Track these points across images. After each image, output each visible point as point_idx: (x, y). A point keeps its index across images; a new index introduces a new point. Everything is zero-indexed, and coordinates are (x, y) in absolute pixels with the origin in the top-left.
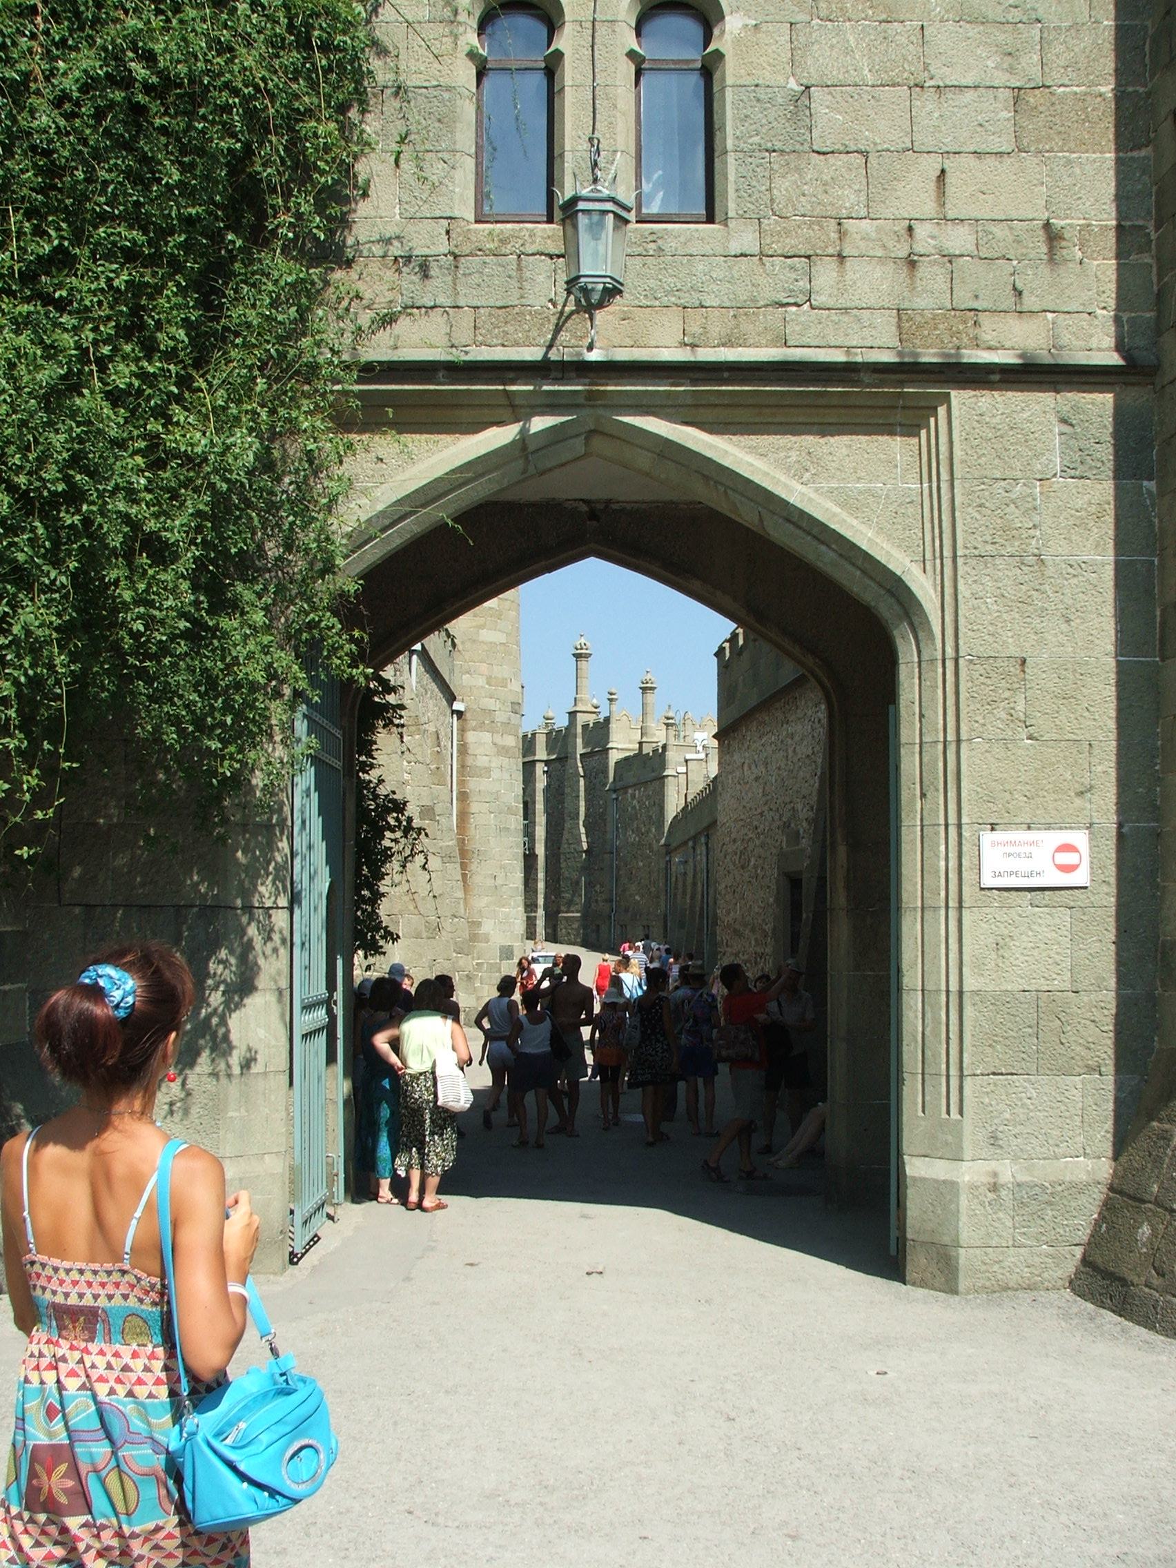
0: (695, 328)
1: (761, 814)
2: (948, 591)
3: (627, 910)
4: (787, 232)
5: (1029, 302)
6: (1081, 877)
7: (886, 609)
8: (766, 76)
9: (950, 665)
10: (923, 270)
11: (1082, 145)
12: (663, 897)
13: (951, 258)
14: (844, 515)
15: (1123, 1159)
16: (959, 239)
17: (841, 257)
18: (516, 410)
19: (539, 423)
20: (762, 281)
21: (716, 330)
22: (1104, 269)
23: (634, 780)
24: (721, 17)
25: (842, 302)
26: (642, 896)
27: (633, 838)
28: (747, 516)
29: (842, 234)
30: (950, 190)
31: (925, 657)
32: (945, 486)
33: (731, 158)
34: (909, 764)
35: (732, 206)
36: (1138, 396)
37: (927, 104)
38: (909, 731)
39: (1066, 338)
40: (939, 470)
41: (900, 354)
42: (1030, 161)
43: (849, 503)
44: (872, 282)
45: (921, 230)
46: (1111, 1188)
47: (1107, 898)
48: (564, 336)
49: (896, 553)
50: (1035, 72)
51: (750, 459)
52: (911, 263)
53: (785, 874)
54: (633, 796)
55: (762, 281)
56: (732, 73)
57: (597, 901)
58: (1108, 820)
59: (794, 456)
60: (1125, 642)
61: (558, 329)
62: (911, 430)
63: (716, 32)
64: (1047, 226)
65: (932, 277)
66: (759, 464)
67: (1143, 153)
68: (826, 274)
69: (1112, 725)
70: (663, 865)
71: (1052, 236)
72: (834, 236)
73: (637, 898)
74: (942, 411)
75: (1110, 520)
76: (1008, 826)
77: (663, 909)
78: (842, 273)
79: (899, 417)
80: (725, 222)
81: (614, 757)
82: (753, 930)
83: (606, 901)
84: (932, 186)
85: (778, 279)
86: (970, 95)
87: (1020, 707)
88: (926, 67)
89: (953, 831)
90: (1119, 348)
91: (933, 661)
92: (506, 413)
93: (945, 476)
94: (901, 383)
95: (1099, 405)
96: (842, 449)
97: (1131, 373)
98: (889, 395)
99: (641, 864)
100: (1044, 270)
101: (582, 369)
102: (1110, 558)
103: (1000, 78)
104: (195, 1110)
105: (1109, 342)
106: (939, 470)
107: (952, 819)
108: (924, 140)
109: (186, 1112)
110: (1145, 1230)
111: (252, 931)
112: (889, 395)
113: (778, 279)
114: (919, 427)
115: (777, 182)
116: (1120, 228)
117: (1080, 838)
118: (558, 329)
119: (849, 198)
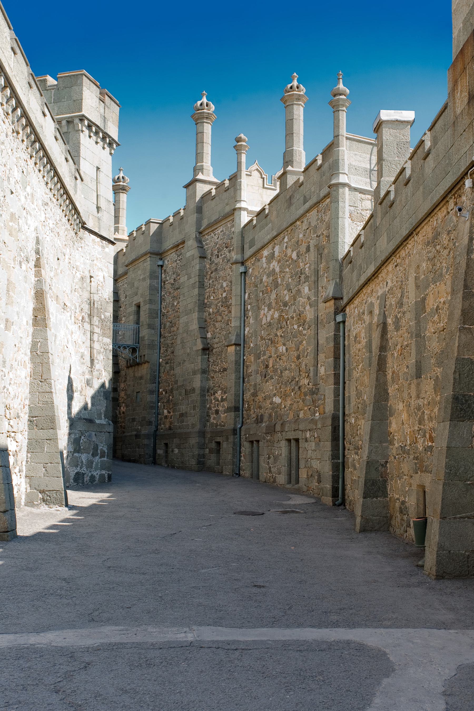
3: (259, 420)
12: (328, 390)
23: (269, 237)
26: (284, 396)
27: (268, 315)
54: (272, 257)
57: (217, 412)
70: (326, 333)
73: (277, 400)
77: (329, 408)
81: (245, 218)
83: (228, 410)
99: (282, 349)
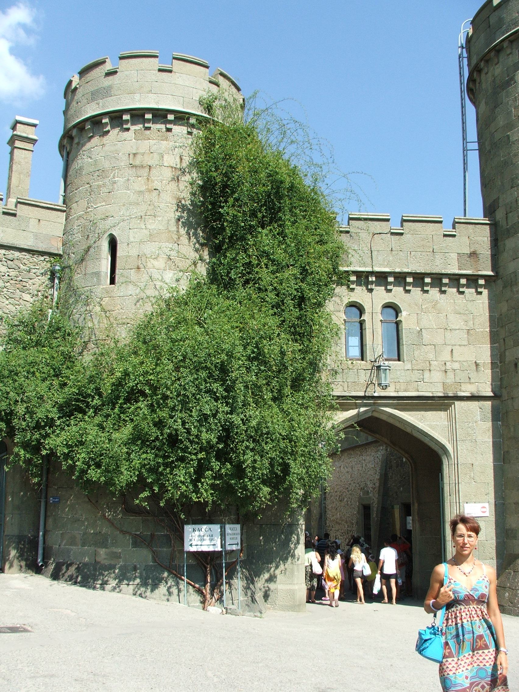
0: (398, 387)
1: (350, 484)
2: (455, 448)
4: (418, 364)
5: (472, 380)
6: (487, 514)
7: (440, 452)
8: (412, 327)
9: (456, 465)
10: (448, 373)
11: (483, 343)
13: (454, 370)
14: (431, 431)
15: (499, 579)
16: (456, 366)
17: (430, 370)
18: (357, 406)
19: (362, 409)
20: (412, 376)
21: (403, 388)
22: (489, 372)
24: (401, 312)
25: (430, 381)
28: (409, 430)
29: (430, 365)
30: (454, 354)
31: (450, 463)
32: (454, 424)
33: (405, 346)
34: (446, 489)
35: (405, 358)
36: (497, 402)
37: (448, 334)
38: (446, 480)
39: (480, 389)
40: (452, 420)
41: (444, 393)
42: (472, 347)
43: (431, 426)
44: (437, 376)
45: (447, 364)
46: (497, 586)
47: (493, 519)
48: (368, 389)
49: (443, 439)
50: (472, 326)
51: (409, 417)
52: (446, 372)
53: (362, 504)
55: (412, 376)
56: (404, 326)
58: (492, 501)
59: (419, 416)
60: (495, 459)
61: (367, 388)
62: (445, 410)
63: (400, 315)
64: (476, 362)
65: (450, 375)
66: (412, 418)
67: (496, 345)
68: (427, 374)
69: (493, 479)
71: (477, 365)
72: (428, 365)
74: (453, 406)
75: (491, 431)
76: (470, 502)
78: (430, 374)
79: (443, 407)
80: (404, 362)
82: (346, 522)
84: (450, 353)
85: (416, 375)
86: (458, 331)
87: (472, 475)
88: (448, 324)
89: (458, 504)
90: (492, 391)
91: (452, 464)
92: (355, 407)
93: (454, 421)
94: (444, 400)
95: (488, 404)
96: (430, 414)
97: (496, 397)
98: (441, 403)
100: (475, 373)
101: (373, 397)
102: (491, 440)
103: (464, 327)
104: (287, 573)
105: (490, 390)
106: (452, 420)
107: (458, 501)
108: (448, 342)
109: (285, 573)
110: (507, 594)
111: (299, 530)
112: (441, 403)
113: (416, 375)
114: (447, 409)
115: (415, 352)
116: (491, 362)
117: (487, 505)
118: (367, 388)
119: (431, 356)
